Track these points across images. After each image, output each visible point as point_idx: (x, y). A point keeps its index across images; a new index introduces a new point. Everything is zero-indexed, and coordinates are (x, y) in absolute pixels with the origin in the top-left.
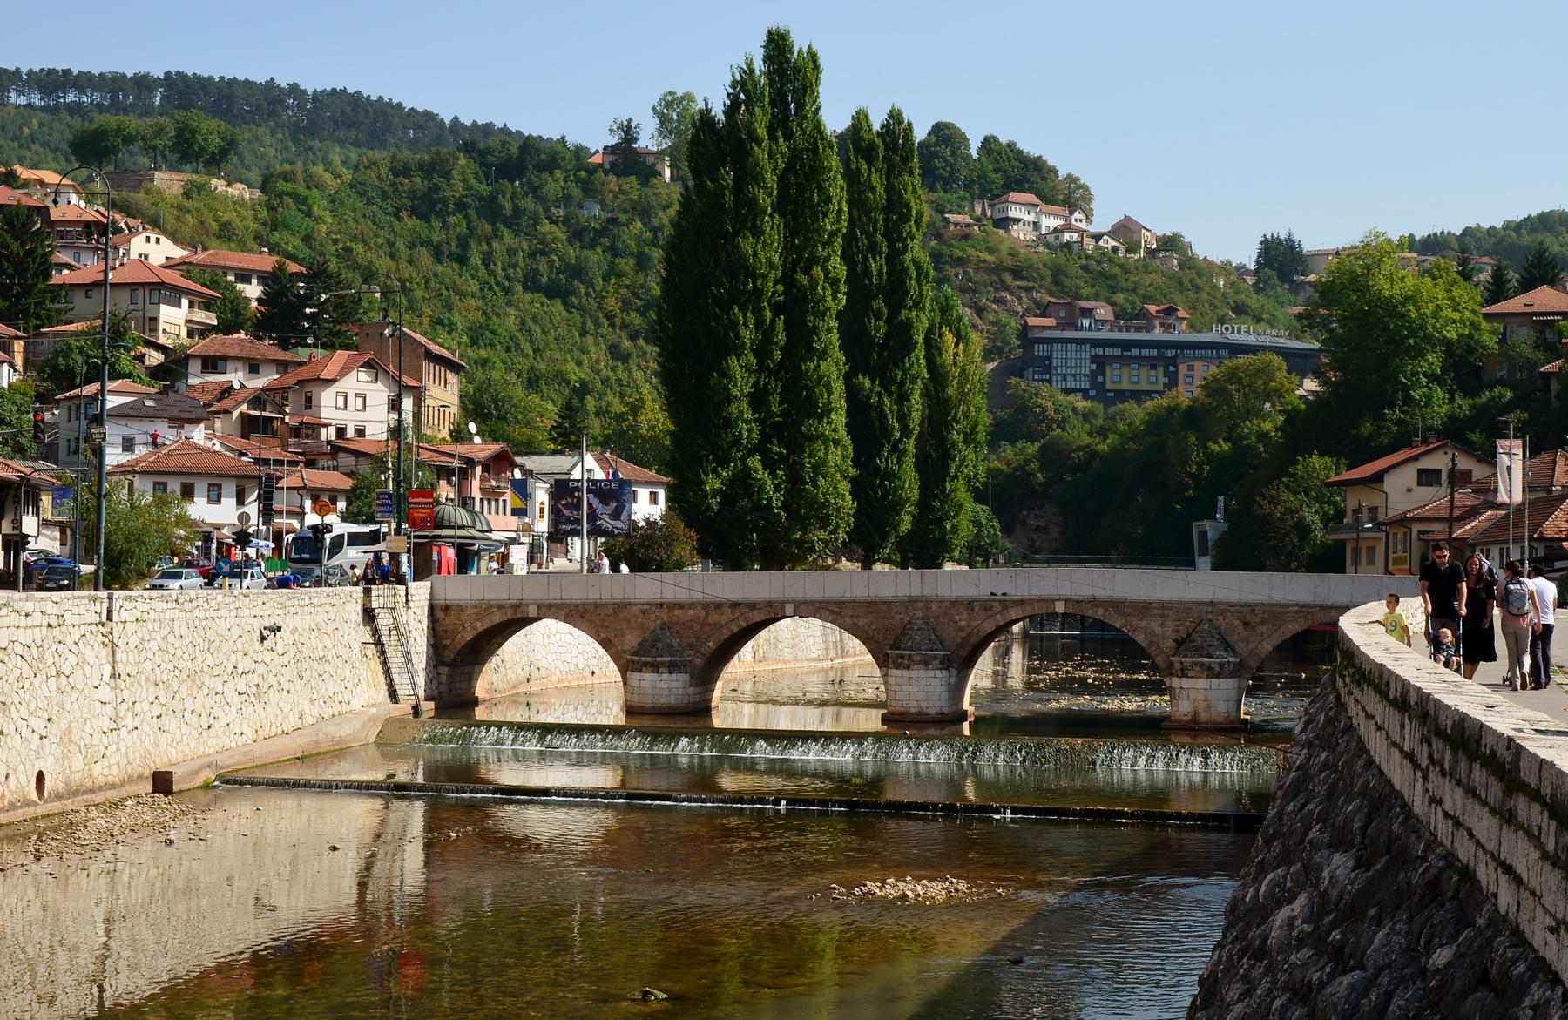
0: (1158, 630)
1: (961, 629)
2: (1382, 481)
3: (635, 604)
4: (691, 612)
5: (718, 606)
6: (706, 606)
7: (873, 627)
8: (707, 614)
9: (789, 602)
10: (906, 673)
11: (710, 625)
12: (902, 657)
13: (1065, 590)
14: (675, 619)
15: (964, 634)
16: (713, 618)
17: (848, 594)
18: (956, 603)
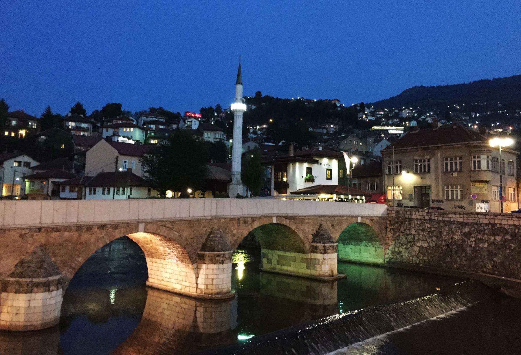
0: (307, 230)
1: (234, 235)
2: (3, 164)
3: (14, 230)
4: (66, 234)
5: (89, 228)
6: (79, 228)
7: (191, 237)
8: (80, 235)
9: (142, 222)
10: (221, 266)
11: (81, 243)
12: (219, 256)
13: (276, 211)
14: (52, 241)
15: (235, 238)
16: (85, 236)
17: (178, 216)
18: (232, 219)
